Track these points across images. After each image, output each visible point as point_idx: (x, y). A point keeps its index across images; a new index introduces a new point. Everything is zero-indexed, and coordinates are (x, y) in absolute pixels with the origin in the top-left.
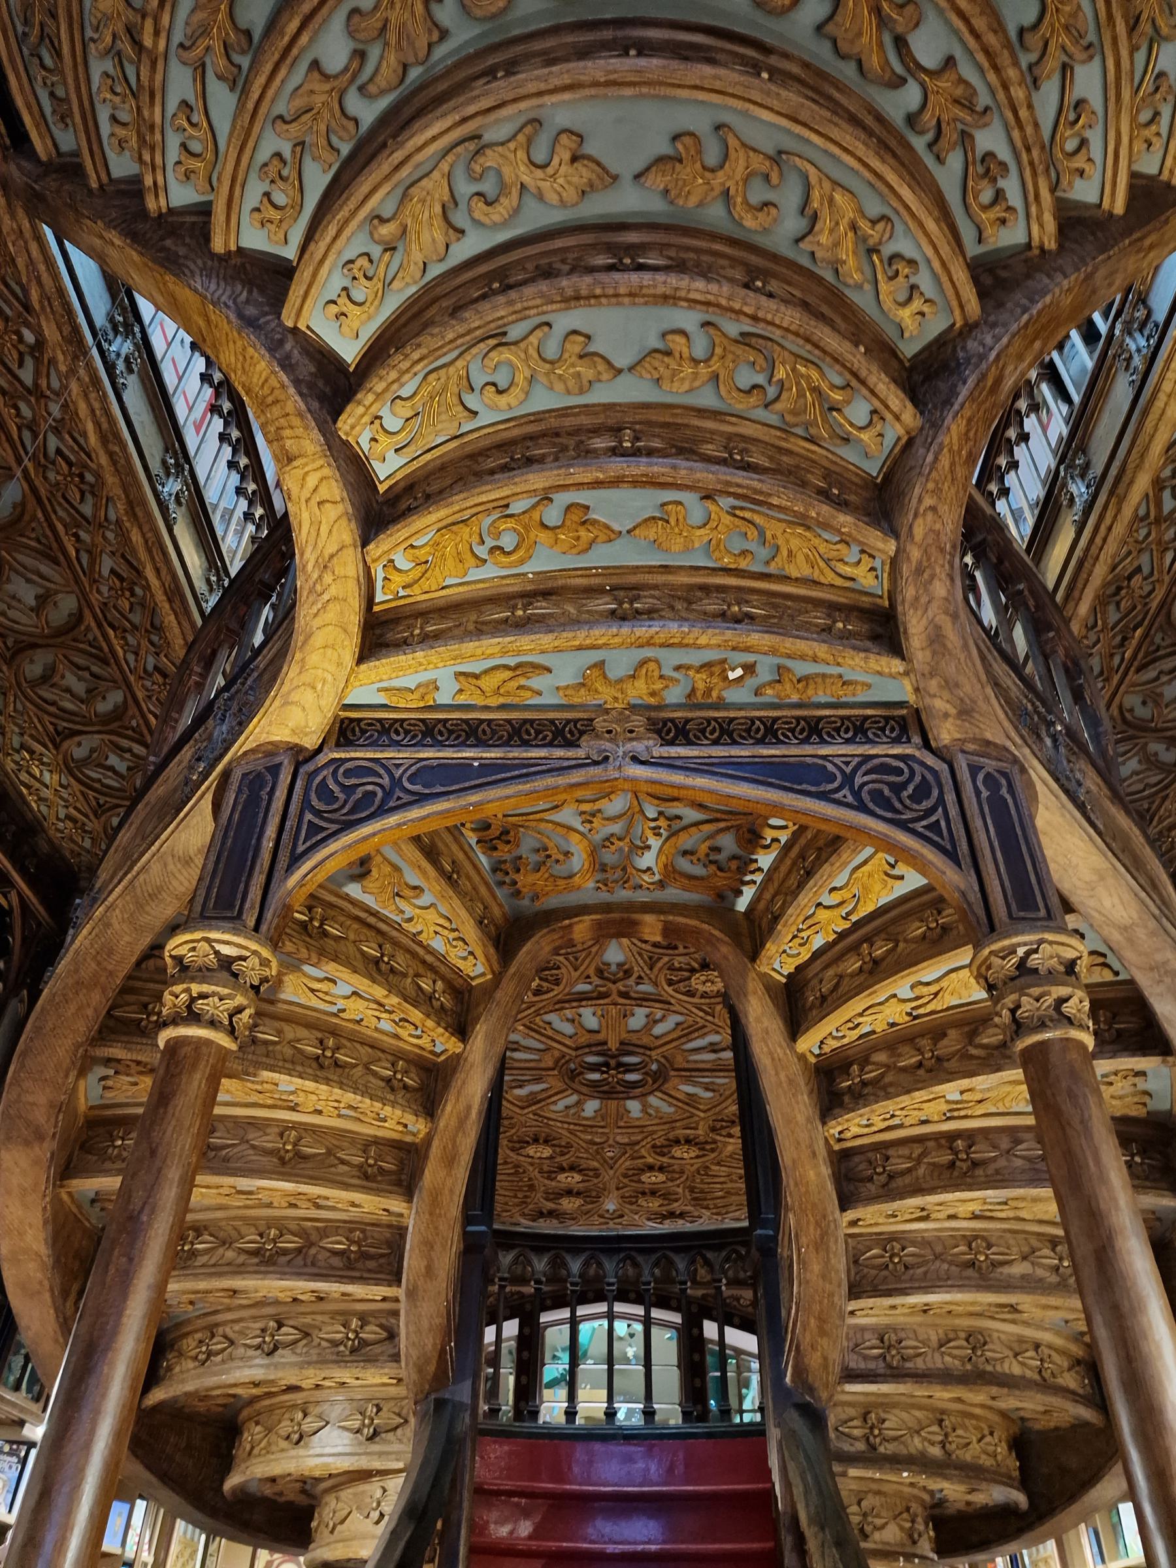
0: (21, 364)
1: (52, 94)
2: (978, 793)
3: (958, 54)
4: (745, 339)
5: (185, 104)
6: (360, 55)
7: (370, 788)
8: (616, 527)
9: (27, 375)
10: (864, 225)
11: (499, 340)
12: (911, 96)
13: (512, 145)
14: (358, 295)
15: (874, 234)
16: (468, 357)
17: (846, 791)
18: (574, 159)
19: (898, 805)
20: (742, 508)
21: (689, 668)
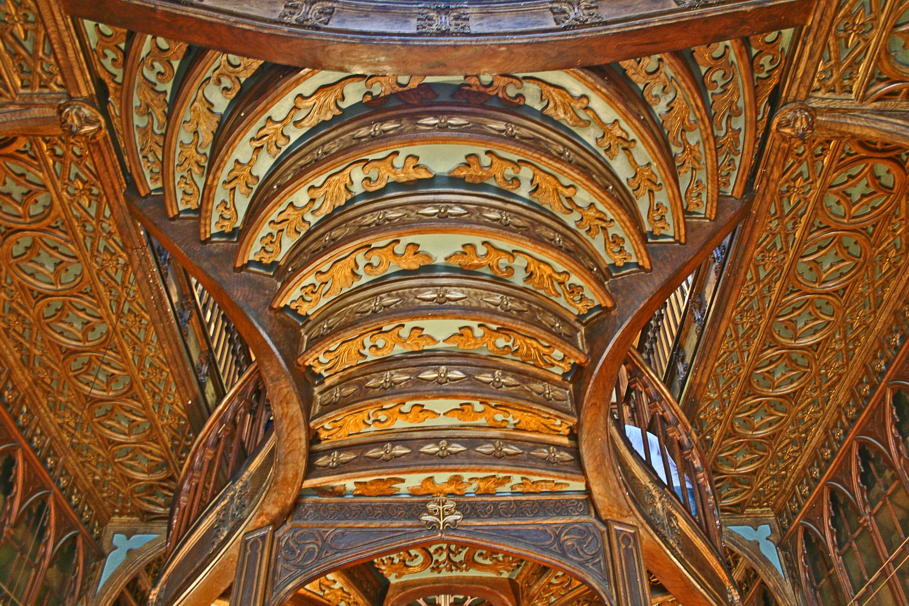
0: (116, 273)
1: (151, 171)
2: (619, 546)
3: (594, 200)
4: (498, 330)
5: (224, 202)
6: (313, 200)
7: (311, 546)
8: (438, 412)
9: (118, 278)
10: (554, 275)
11: (380, 330)
12: (576, 216)
13: (385, 249)
14: (308, 298)
15: (561, 278)
16: (362, 337)
17: (556, 545)
18: (415, 253)
19: (581, 553)
20: (501, 406)
21: (476, 479)
